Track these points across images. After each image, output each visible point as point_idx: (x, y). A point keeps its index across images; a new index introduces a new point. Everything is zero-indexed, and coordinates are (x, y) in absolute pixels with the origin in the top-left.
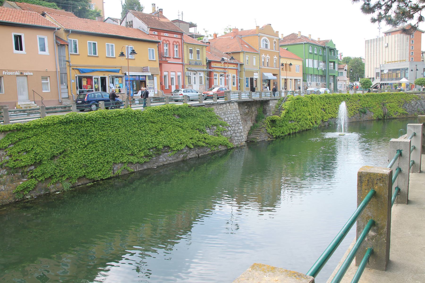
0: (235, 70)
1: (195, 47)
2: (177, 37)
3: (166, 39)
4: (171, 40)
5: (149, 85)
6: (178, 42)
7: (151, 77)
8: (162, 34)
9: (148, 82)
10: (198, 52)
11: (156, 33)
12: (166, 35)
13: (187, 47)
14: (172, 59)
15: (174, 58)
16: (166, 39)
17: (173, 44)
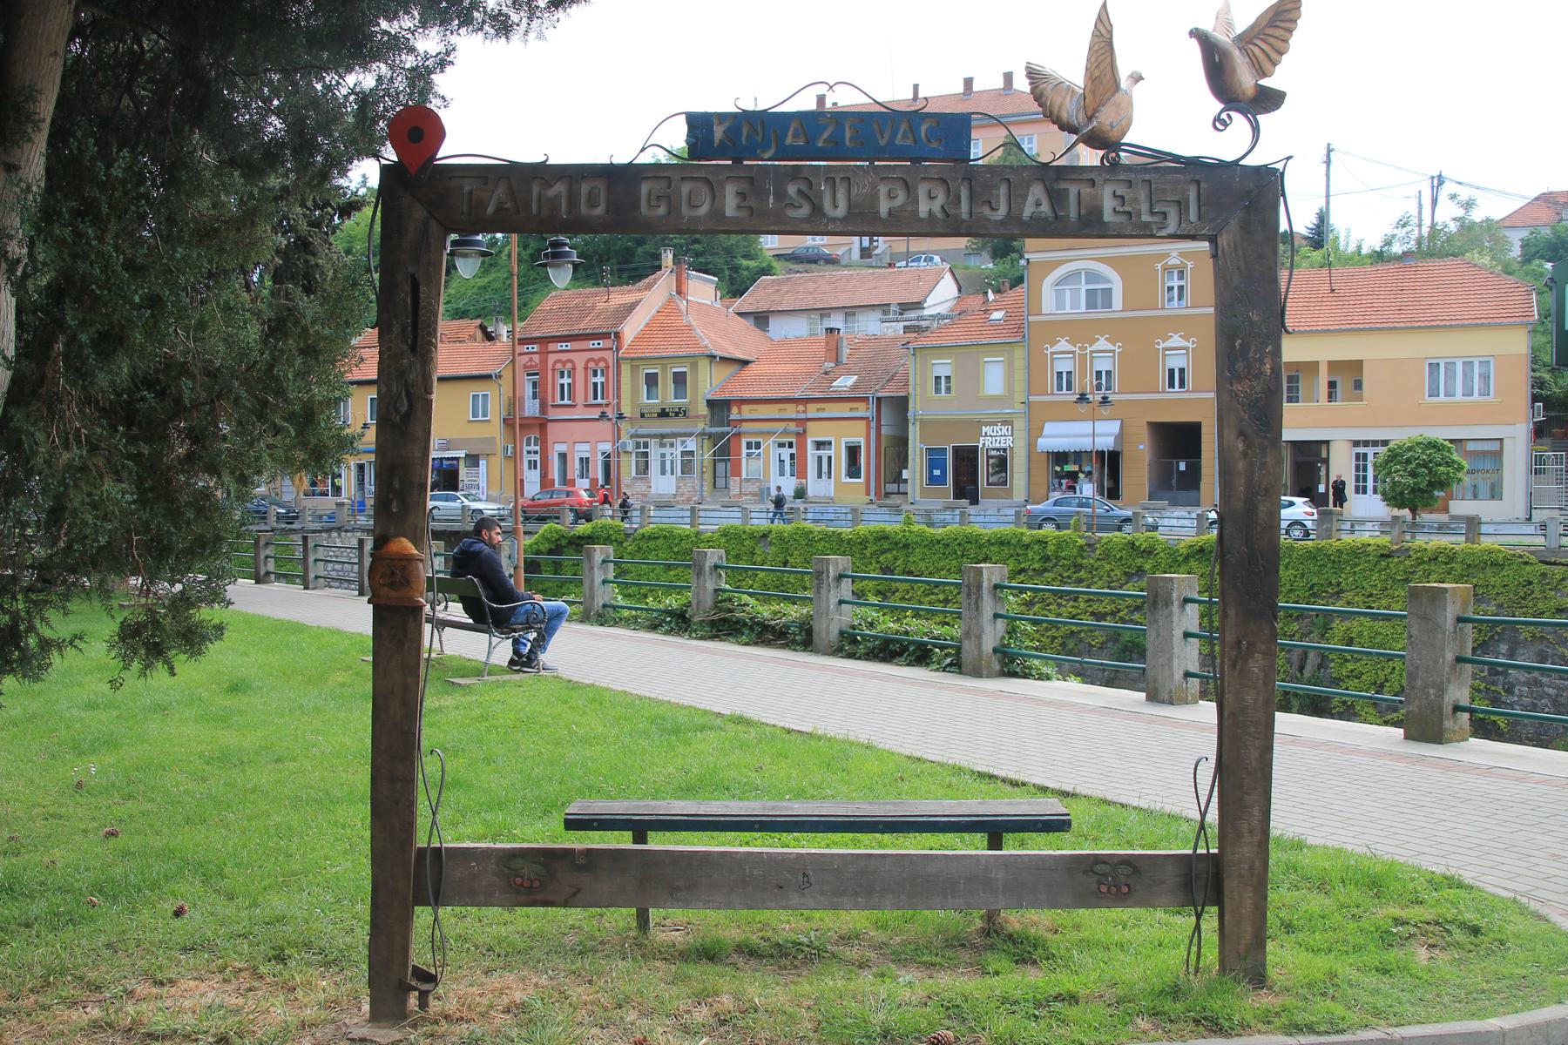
0: (863, 423)
1: (664, 367)
2: (601, 346)
3: (564, 357)
4: (580, 360)
5: (466, 479)
6: (602, 359)
7: (473, 460)
8: (552, 347)
9: (463, 473)
10: (680, 379)
11: (536, 348)
12: (564, 348)
13: (634, 369)
14: (580, 408)
15: (586, 406)
16: (564, 357)
17: (586, 368)
